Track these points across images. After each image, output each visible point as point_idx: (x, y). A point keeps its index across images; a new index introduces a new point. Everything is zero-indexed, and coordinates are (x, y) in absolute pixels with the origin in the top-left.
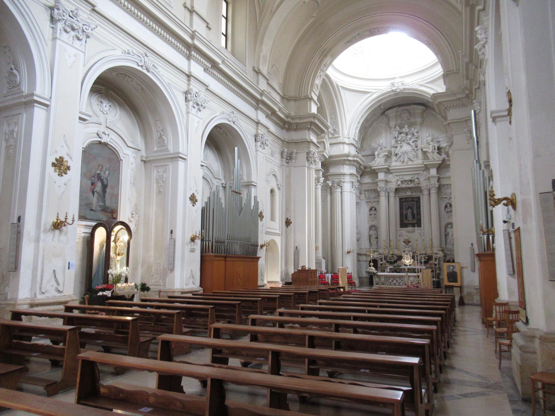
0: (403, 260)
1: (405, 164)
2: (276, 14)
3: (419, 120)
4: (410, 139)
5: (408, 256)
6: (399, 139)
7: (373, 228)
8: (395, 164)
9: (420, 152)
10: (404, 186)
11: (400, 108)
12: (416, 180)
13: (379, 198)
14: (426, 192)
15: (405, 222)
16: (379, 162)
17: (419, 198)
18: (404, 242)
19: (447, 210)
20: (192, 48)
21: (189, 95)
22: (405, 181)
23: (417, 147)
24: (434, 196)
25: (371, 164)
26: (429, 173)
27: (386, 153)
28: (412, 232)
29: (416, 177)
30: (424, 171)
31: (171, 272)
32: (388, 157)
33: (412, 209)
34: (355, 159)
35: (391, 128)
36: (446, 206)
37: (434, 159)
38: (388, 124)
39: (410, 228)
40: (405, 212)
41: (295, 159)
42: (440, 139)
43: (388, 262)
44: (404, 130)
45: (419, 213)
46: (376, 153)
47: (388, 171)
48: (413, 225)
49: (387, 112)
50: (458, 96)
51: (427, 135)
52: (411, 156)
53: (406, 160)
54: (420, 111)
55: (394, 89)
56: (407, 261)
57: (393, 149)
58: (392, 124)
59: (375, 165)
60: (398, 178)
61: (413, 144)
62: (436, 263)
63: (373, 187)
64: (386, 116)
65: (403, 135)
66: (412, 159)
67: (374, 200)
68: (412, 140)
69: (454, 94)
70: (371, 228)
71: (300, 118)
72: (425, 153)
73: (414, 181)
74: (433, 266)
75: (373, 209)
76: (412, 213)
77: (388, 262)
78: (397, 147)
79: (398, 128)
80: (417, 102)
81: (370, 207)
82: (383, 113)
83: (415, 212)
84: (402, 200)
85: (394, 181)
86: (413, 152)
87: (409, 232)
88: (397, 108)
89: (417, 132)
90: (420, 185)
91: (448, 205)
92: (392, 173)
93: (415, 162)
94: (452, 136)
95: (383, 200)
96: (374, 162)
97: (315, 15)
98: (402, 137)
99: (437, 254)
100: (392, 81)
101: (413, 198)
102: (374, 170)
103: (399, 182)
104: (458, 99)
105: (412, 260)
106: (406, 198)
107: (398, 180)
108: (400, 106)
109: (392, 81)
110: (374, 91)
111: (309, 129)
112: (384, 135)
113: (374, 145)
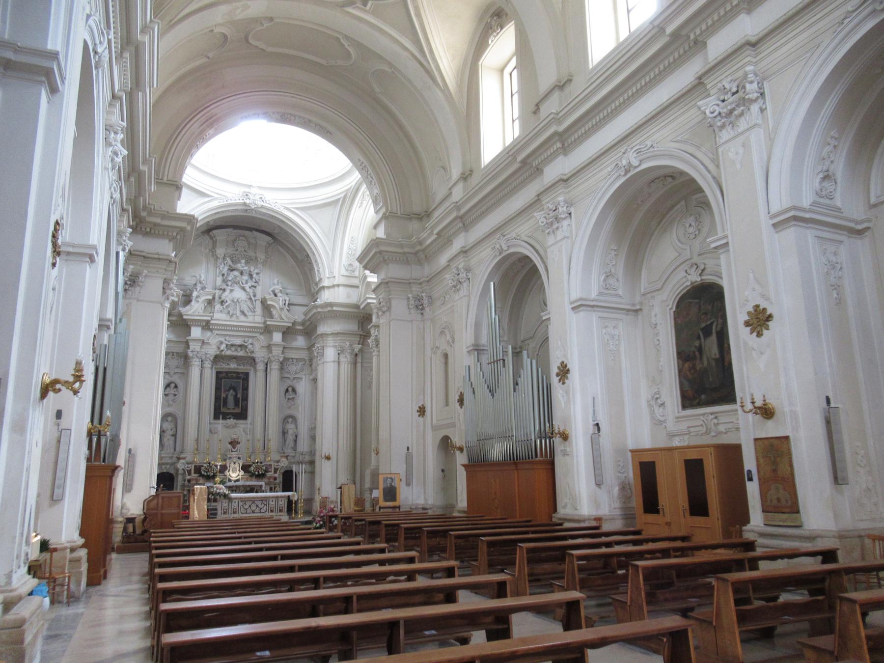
0: (227, 473)
1: (234, 318)
2: (177, 28)
3: (261, 256)
4: (247, 283)
5: (237, 465)
7: (170, 419)
8: (219, 316)
9: (258, 305)
10: (229, 353)
11: (235, 231)
12: (250, 346)
14: (261, 367)
15: (223, 410)
16: (195, 310)
17: (247, 375)
18: (230, 443)
19: (288, 396)
20: (133, 49)
21: (112, 135)
22: (232, 345)
23: (254, 296)
24: (274, 376)
25: (183, 310)
26: (271, 337)
27: (211, 297)
28: (234, 427)
30: (261, 333)
31: (50, 506)
32: (210, 303)
33: (235, 390)
35: (217, 257)
36: (287, 390)
37: (282, 318)
38: (213, 250)
39: (231, 421)
40: (223, 395)
41: (141, 287)
42: (288, 291)
43: (203, 476)
44: (239, 266)
45: (245, 398)
46: (195, 294)
47: (207, 326)
49: (215, 232)
50: (406, 250)
51: (276, 281)
52: (245, 308)
53: (238, 313)
54: (265, 244)
55: (248, 201)
56: (235, 474)
57: (218, 292)
58: (220, 252)
59: (190, 313)
60: (222, 339)
61: (250, 291)
62: (276, 475)
63: (179, 349)
64: (211, 238)
65: (236, 273)
66: (246, 312)
67: (177, 370)
68: (249, 284)
69: (401, 246)
70: (165, 418)
71: (164, 217)
72: (267, 309)
73: (246, 347)
74: (272, 480)
75: (173, 385)
76: (235, 397)
77: (201, 475)
78: (224, 290)
79: (228, 260)
80: (263, 228)
81: (167, 382)
83: (239, 396)
85: (214, 344)
86: (249, 303)
87: (228, 427)
89: (257, 274)
90: (254, 355)
91: (290, 389)
92: (211, 330)
93: (250, 319)
94: (390, 299)
95: (195, 372)
96: (188, 307)
97: (210, 55)
98: (236, 277)
99: (278, 462)
100: (247, 190)
101: (238, 373)
102: (185, 320)
103: (223, 347)
104: (404, 253)
105: (242, 473)
106: (227, 373)
107: (222, 343)
108: (235, 227)
109: (247, 190)
110: (217, 196)
111: (172, 239)
112: (204, 266)
113: (189, 280)
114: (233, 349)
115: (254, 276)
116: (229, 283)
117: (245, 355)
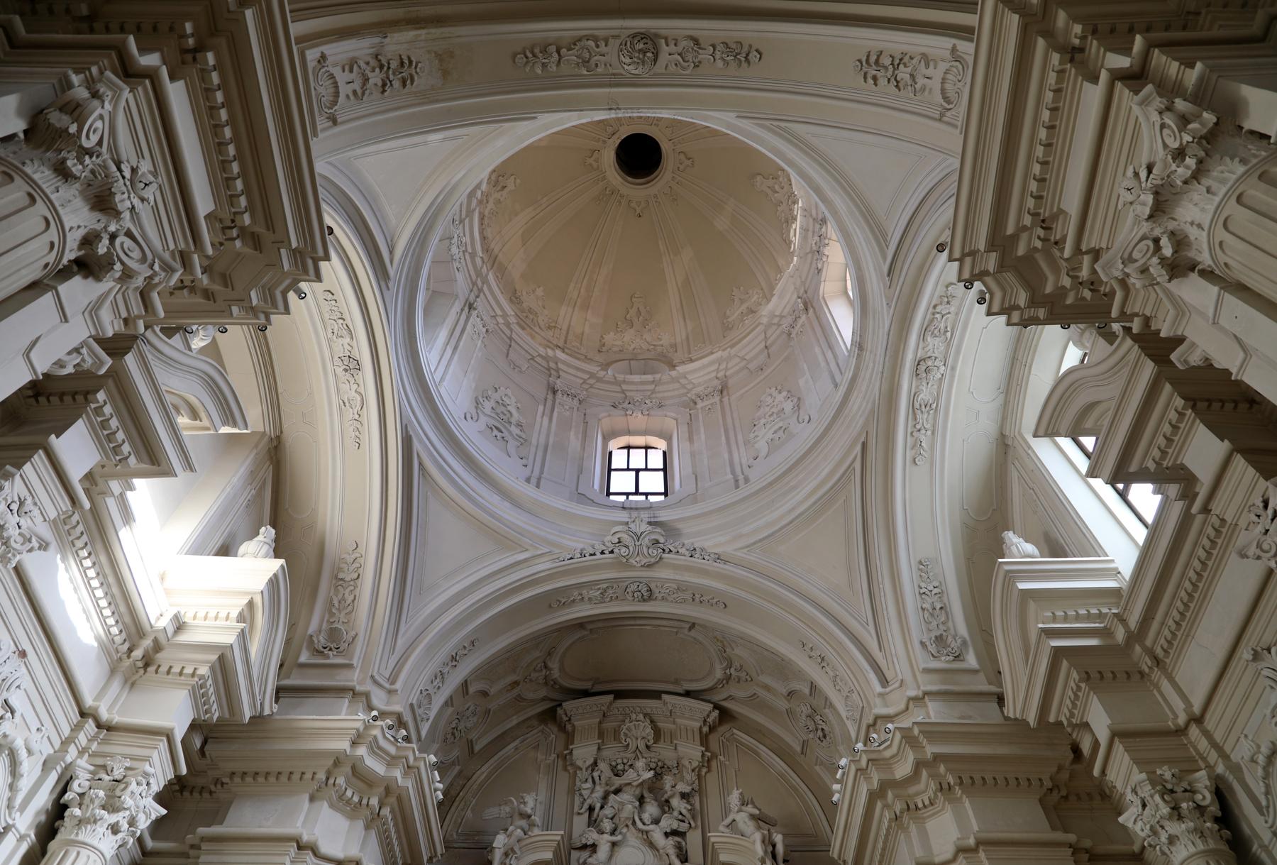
4: (656, 821)
6: (608, 811)
34: (397, 773)
38: (565, 758)
44: (630, 775)
58: (583, 753)
64: (562, 728)
78: (593, 848)
82: (550, 715)
88: (611, 697)
115: (676, 802)
116: (607, 825)
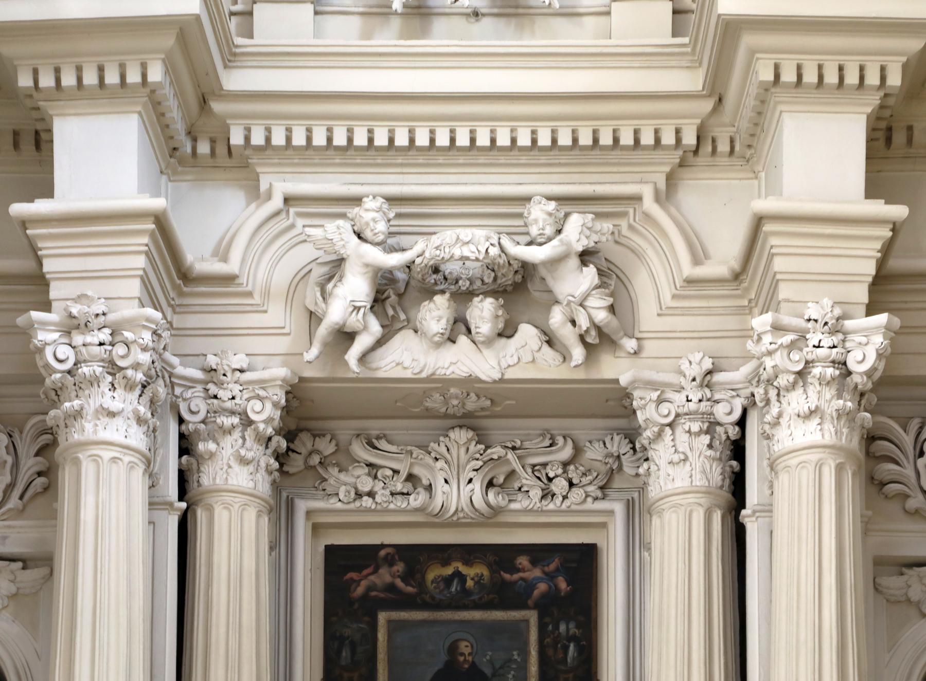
13: (52, 515)
14: (680, 472)
22: (430, 280)
29: (577, 231)
48: (364, 556)
60: (337, 232)
84: (364, 584)
90: (616, 368)
92: (236, 164)
107: (337, 265)
114: (435, 314)
117: (547, 367)
